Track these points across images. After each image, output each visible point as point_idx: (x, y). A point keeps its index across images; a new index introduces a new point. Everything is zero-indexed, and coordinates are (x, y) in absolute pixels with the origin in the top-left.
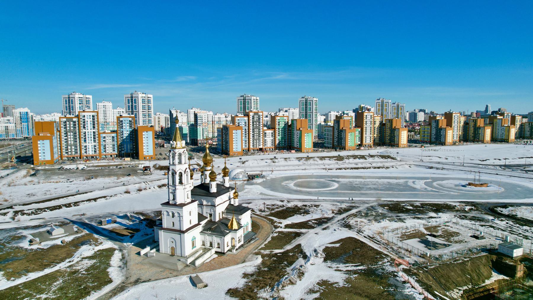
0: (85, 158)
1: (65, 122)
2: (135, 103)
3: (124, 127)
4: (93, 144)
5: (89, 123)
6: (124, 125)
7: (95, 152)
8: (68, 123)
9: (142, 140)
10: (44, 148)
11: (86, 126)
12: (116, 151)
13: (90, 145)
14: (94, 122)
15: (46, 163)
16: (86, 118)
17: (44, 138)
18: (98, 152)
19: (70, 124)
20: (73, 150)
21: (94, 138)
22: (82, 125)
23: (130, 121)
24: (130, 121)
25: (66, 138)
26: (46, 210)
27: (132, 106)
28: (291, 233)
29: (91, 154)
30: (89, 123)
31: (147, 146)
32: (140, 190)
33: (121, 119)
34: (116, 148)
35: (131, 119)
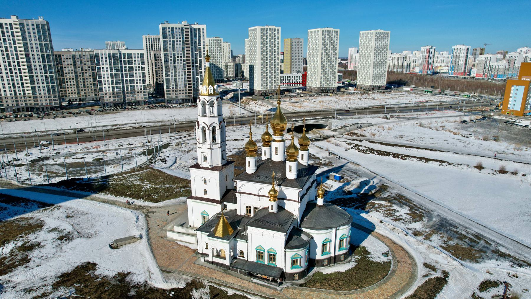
10: (516, 95)
17: (518, 83)
26: (375, 152)
32: (503, 171)
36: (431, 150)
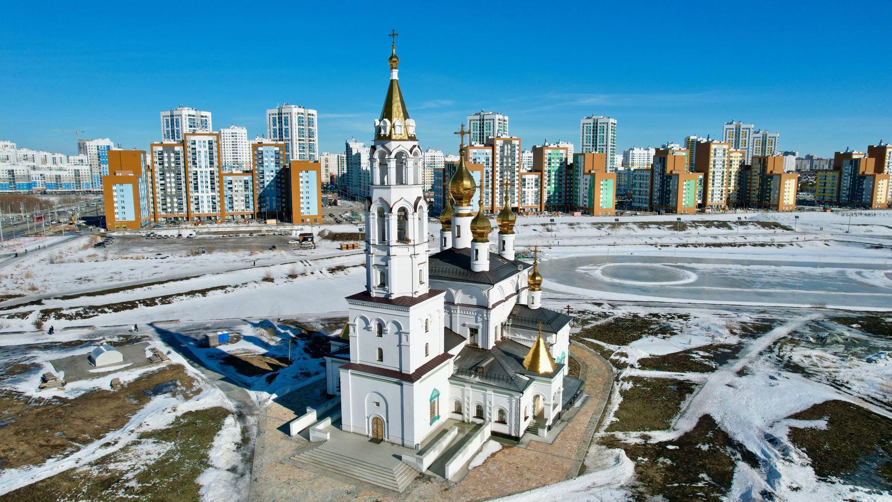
0: (196, 219)
1: (161, 153)
2: (286, 124)
3: (266, 164)
4: (211, 194)
5: (203, 155)
6: (265, 159)
7: (214, 208)
8: (166, 155)
9: (299, 187)
10: (122, 199)
11: (197, 161)
12: (252, 207)
13: (205, 195)
14: (211, 154)
15: (128, 225)
16: (197, 146)
17: (123, 181)
18: (218, 209)
19: (169, 157)
20: (176, 205)
21: (212, 183)
22: (190, 159)
23: (277, 153)
24: (277, 153)
25: (163, 182)
26: (106, 310)
27: (281, 129)
28: (665, 381)
29: (206, 212)
30: (203, 155)
31: (308, 198)
32: (293, 276)
33: (260, 149)
34: (251, 202)
35: (277, 149)
36: (182, 280)
